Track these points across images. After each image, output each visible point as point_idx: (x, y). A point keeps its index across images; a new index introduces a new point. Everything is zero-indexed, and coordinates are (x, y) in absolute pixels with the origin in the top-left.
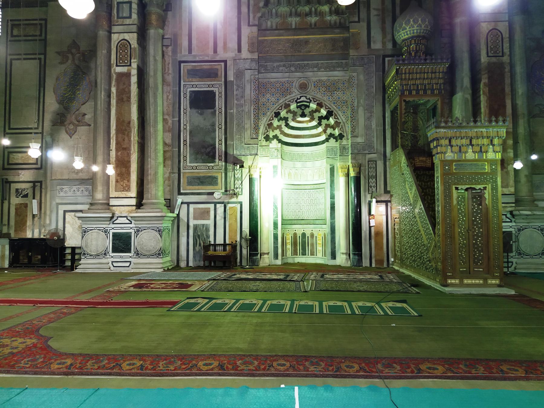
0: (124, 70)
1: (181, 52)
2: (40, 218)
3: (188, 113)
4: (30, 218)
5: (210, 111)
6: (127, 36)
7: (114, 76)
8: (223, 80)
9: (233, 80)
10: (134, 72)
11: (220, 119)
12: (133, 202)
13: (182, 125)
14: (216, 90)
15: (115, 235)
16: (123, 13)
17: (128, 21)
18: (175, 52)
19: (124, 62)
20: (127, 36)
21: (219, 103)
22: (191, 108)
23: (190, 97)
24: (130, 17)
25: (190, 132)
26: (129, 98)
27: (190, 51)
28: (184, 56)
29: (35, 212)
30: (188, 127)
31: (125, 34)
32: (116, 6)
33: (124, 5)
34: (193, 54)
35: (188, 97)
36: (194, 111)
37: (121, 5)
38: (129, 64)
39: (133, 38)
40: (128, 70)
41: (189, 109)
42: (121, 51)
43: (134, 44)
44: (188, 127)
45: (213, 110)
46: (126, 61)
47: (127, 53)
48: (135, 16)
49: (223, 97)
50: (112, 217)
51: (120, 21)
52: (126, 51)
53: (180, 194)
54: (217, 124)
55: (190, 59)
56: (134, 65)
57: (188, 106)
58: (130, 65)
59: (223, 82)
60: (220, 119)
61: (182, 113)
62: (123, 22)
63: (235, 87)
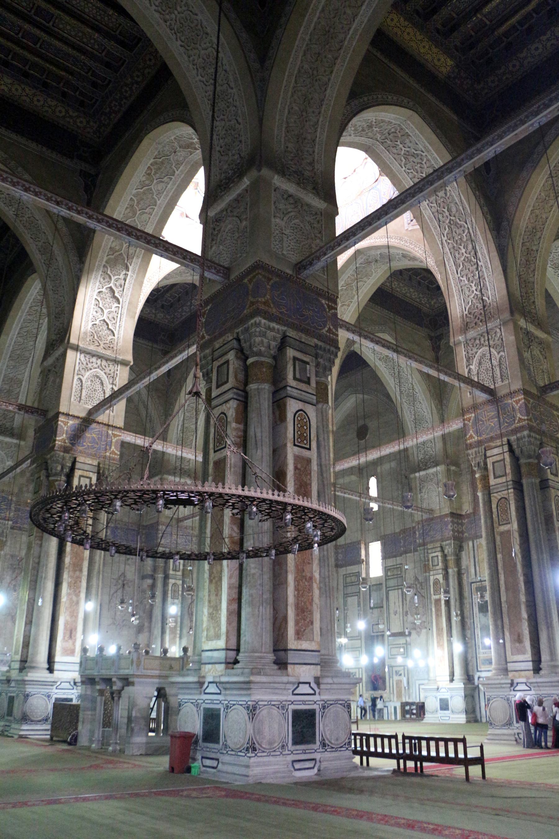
0: (437, 597)
2: (409, 688)
4: (403, 689)
7: (433, 602)
12: (448, 678)
15: (441, 700)
17: (437, 567)
18: (468, 578)
24: (438, 565)
29: (406, 685)
36: (481, 614)
39: (440, 577)
48: (440, 564)
50: (438, 689)
53: (478, 671)
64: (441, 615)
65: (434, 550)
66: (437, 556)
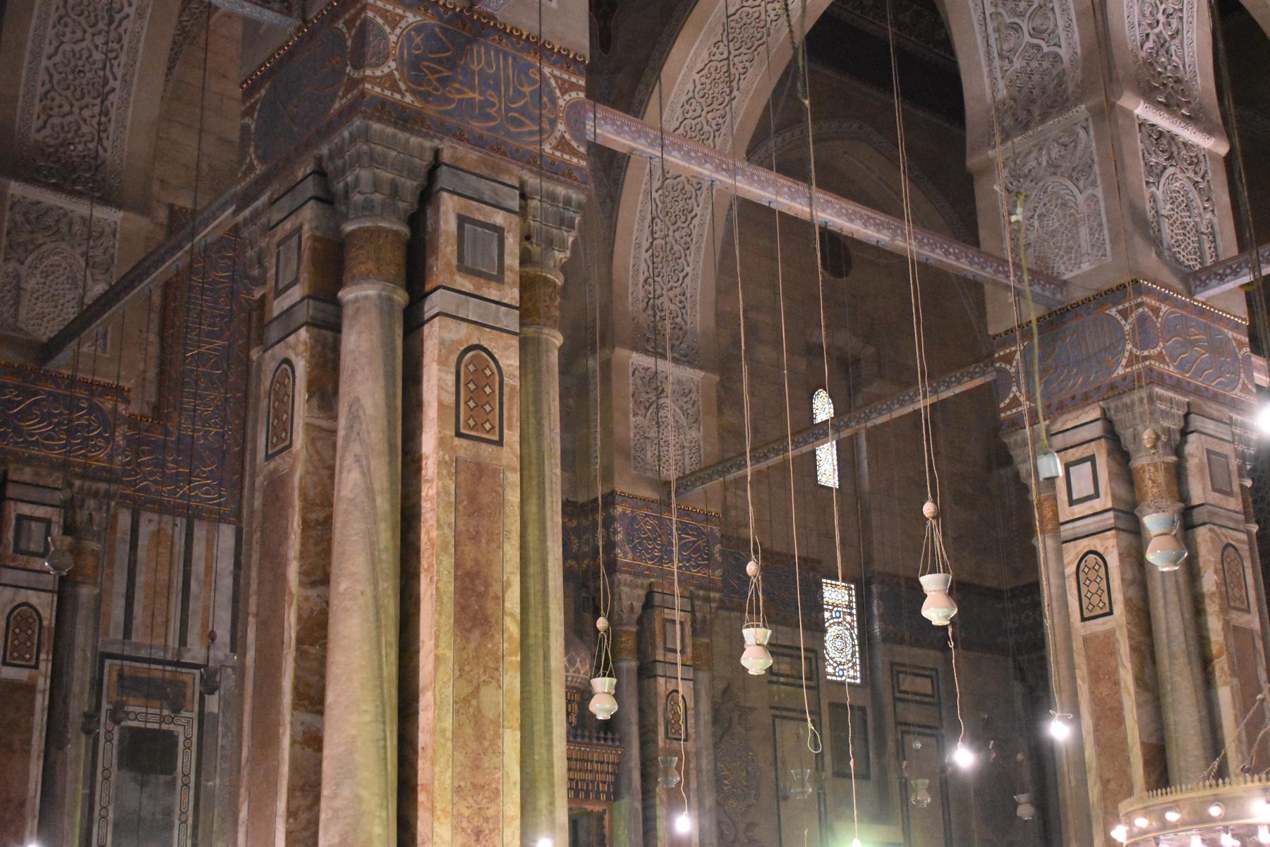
1: (106, 633)
3: (112, 779)
5: (162, 778)
6: (34, 598)
8: (196, 708)
9: (215, 710)
10: (43, 683)
11: (184, 800)
13: (97, 807)
14: (179, 730)
16: (29, 540)
19: (22, 657)
20: (34, 598)
21: (185, 761)
22: (120, 767)
23: (121, 741)
25: (116, 826)
26: (28, 742)
27: (127, 632)
28: (113, 643)
30: (111, 815)
31: (30, 592)
32: (13, 522)
33: (33, 524)
34: (134, 639)
35: (115, 742)
37: (25, 523)
38: (33, 663)
40: (30, 678)
41: (115, 768)
42: (17, 631)
43: (48, 616)
44: (111, 815)
45: (169, 778)
46: (16, 655)
47: (30, 638)
49: (194, 748)
51: (22, 560)
52: (30, 632)
54: (177, 811)
55: (127, 651)
56: (45, 667)
57: (115, 761)
58: (36, 667)
59: (195, 715)
60: (184, 800)
61: (99, 778)
62: (27, 562)
63: (220, 728)
64: (26, 752)
65: (33, 494)
66: (47, 522)
